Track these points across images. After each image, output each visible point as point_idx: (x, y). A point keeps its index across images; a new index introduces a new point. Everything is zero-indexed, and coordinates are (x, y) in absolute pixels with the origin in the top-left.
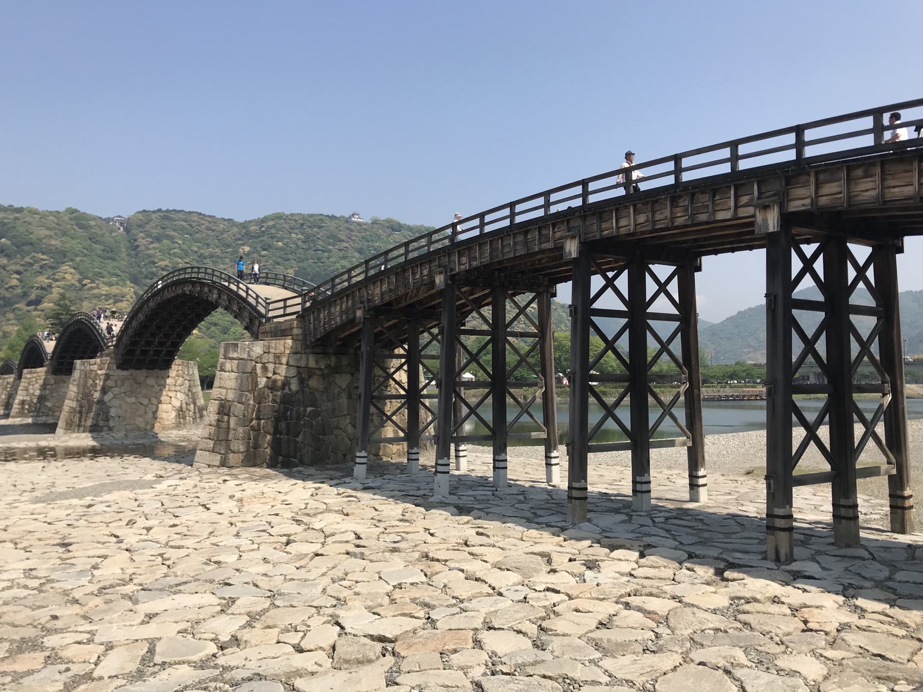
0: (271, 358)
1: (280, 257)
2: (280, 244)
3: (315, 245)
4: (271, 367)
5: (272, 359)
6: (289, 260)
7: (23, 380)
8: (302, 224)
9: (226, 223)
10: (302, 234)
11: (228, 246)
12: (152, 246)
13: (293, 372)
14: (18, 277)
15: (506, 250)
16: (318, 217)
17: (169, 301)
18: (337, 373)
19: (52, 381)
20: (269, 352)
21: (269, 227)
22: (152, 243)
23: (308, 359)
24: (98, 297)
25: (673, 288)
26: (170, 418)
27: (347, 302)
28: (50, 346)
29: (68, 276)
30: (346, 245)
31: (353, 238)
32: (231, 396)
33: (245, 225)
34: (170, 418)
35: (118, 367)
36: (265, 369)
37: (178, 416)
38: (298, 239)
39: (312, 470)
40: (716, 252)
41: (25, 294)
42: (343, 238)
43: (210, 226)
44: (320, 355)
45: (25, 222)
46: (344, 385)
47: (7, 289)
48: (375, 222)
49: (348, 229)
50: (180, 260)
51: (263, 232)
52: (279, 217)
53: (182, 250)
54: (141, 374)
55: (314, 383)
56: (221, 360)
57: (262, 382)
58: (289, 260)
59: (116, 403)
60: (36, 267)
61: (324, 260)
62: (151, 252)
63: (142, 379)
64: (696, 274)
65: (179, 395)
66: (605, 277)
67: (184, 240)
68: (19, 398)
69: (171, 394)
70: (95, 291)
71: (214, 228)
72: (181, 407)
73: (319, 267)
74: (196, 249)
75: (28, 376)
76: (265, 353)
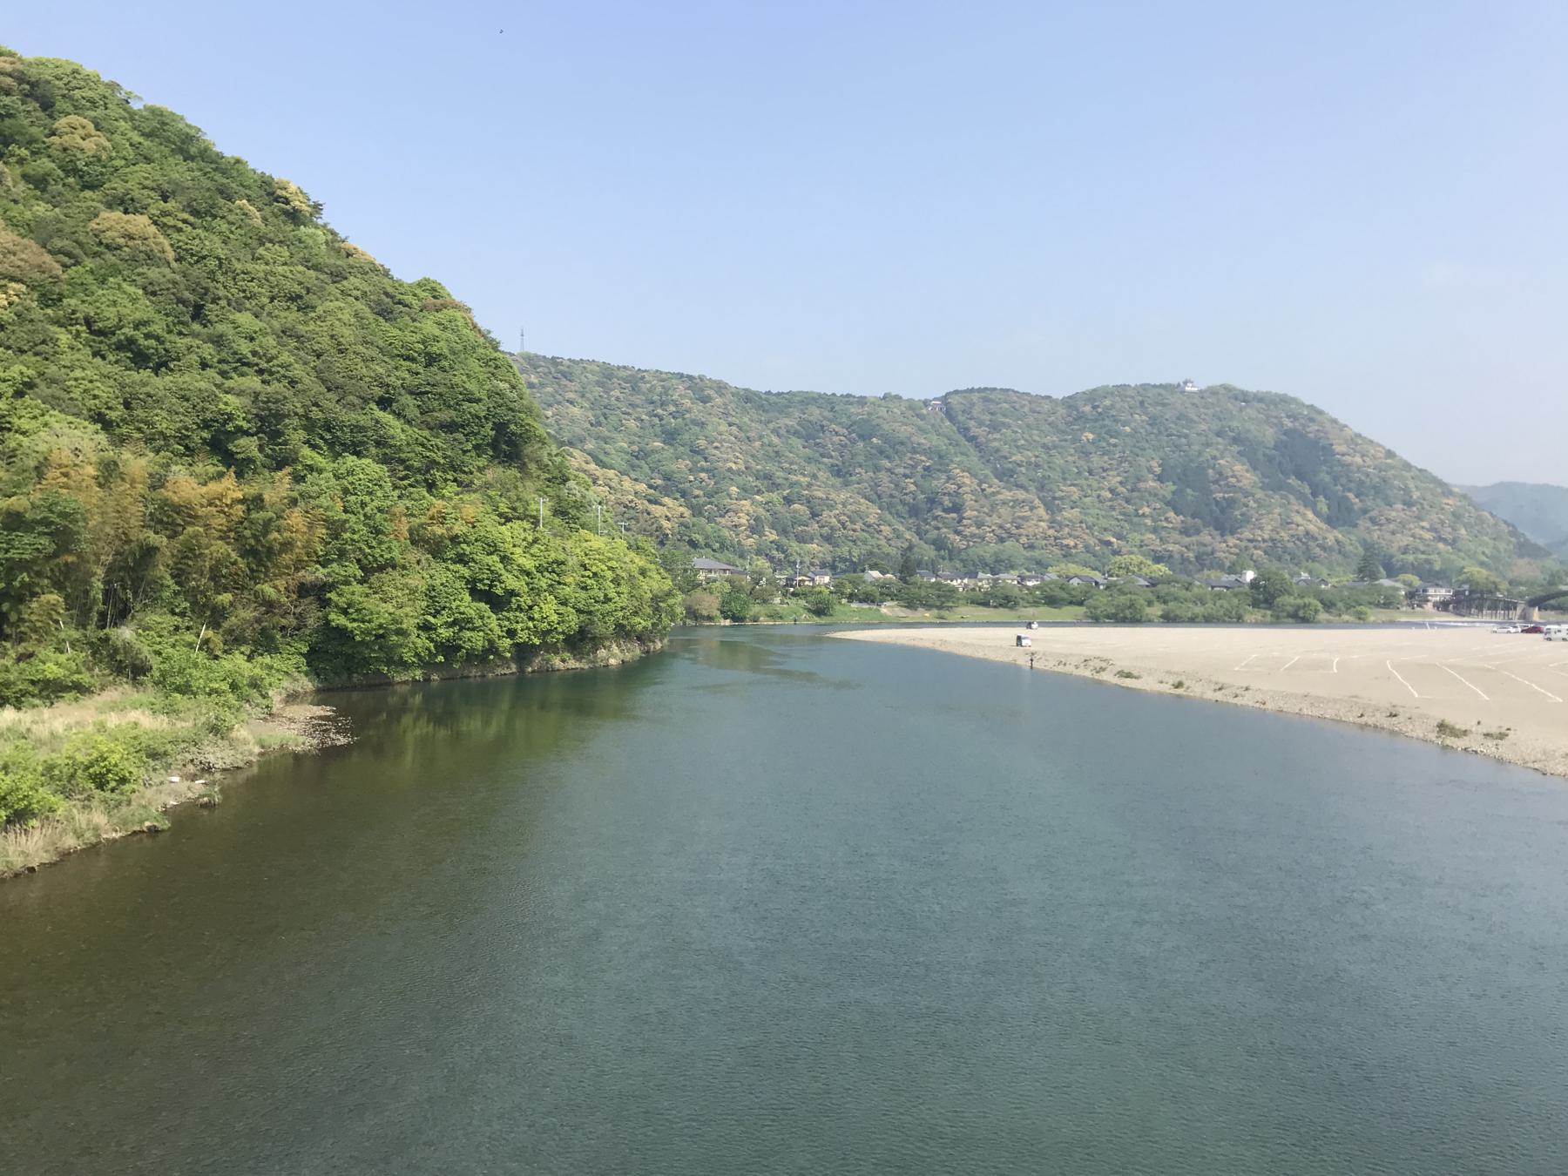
1: (1134, 446)
2: (1128, 429)
3: (1167, 430)
6: (1145, 449)
8: (1142, 403)
9: (1048, 401)
10: (1146, 414)
11: (1064, 432)
12: (990, 436)
14: (912, 481)
16: (1156, 391)
21: (1107, 408)
22: (989, 433)
24: (1004, 503)
29: (967, 481)
30: (1204, 427)
31: (1203, 416)
33: (1070, 402)
38: (1143, 421)
41: (932, 501)
42: (1195, 418)
43: (1033, 406)
45: (878, 417)
47: (906, 494)
48: (1213, 391)
49: (1193, 404)
50: (1029, 453)
51: (1100, 414)
52: (1104, 392)
53: (1026, 440)
58: (1145, 449)
60: (919, 468)
61: (1186, 448)
62: (996, 444)
67: (1019, 427)
70: (1000, 497)
71: (1038, 409)
73: (1180, 456)
74: (1037, 439)
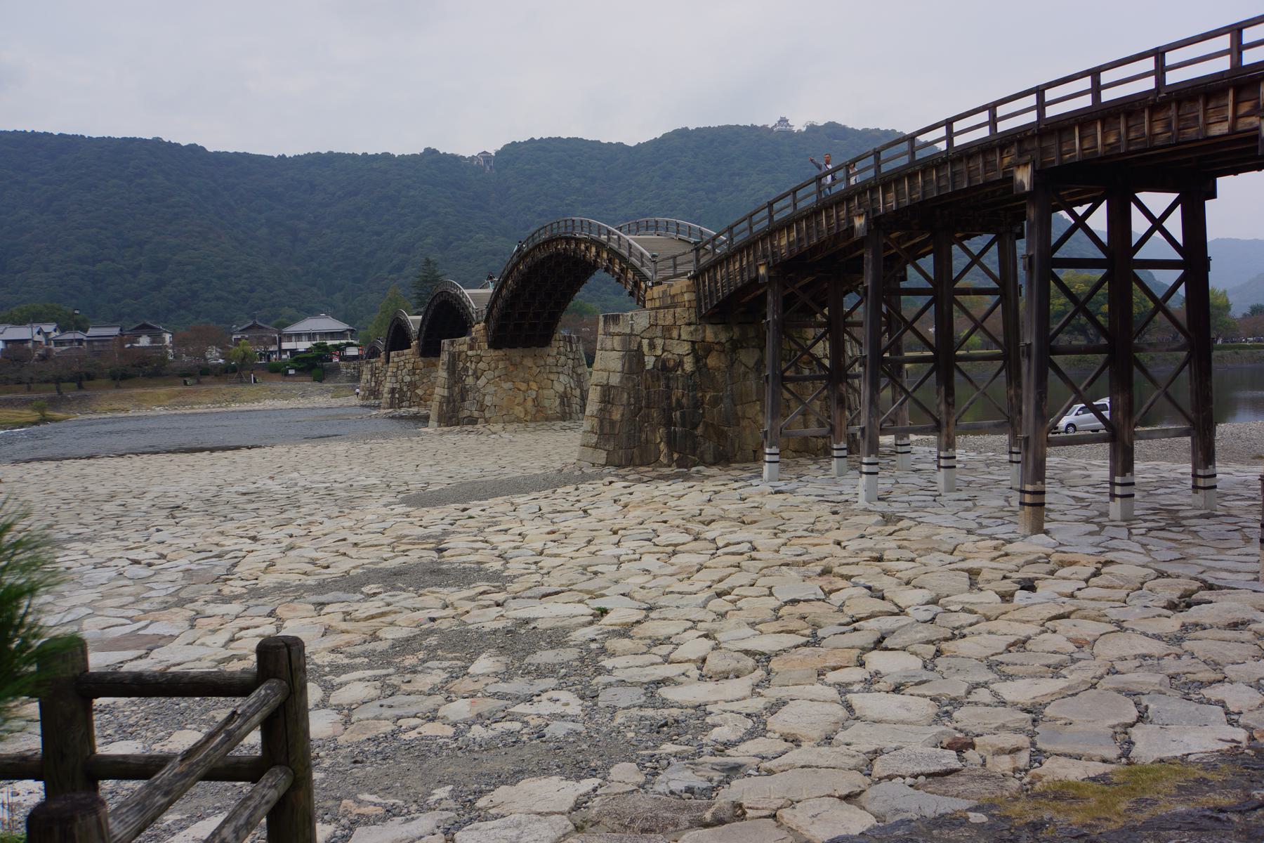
0: (658, 332)
4: (659, 342)
5: (660, 334)
7: (391, 365)
13: (685, 348)
15: (943, 183)
17: (543, 262)
18: (742, 347)
19: (421, 365)
20: (656, 325)
23: (704, 331)
25: (1174, 224)
26: (553, 407)
27: (748, 256)
28: (414, 321)
32: (615, 380)
34: (553, 407)
35: (490, 347)
36: (652, 346)
37: (562, 403)
39: (714, 470)
40: (1235, 172)
44: (720, 326)
46: (751, 363)
48: (812, 129)
54: (516, 354)
55: (712, 361)
56: (600, 337)
57: (650, 361)
59: (491, 389)
63: (518, 359)
64: (1208, 203)
65: (562, 378)
66: (1073, 214)
68: (387, 386)
69: (552, 377)
72: (565, 392)
75: (396, 359)
76: (651, 325)
